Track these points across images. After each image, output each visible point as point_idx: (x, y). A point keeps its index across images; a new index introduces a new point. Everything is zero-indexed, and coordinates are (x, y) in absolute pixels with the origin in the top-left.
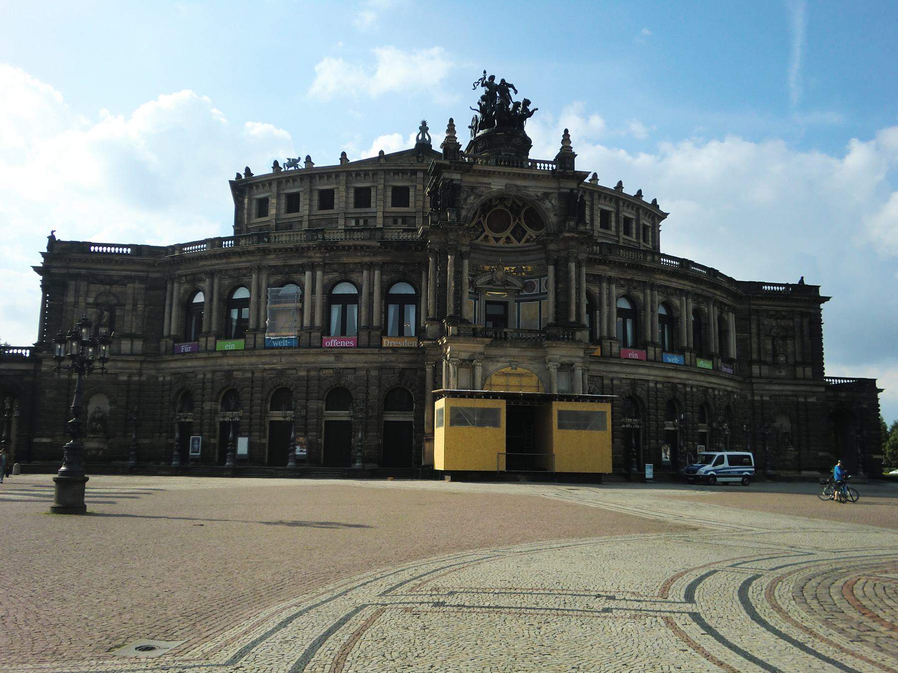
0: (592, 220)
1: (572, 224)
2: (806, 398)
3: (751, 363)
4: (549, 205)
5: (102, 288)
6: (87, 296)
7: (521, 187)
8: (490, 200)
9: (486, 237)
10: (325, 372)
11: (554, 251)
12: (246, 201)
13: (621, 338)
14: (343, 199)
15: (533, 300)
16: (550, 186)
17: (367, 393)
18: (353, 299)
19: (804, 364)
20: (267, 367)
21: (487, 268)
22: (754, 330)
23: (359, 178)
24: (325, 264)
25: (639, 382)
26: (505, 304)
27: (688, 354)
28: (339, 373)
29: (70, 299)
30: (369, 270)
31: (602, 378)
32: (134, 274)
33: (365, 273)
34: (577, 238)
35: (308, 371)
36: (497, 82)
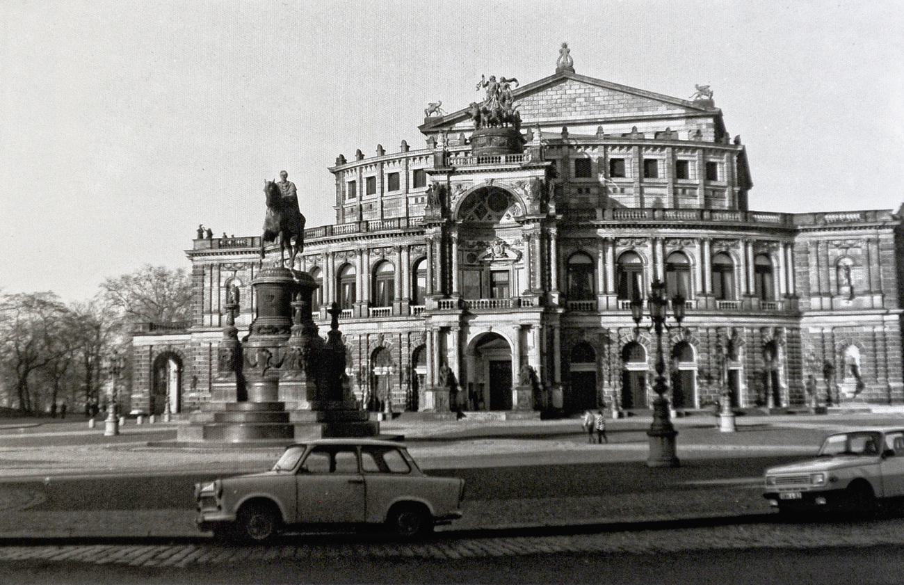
1: (537, 208)
2: (874, 328)
3: (810, 295)
4: (520, 191)
5: (230, 274)
6: (219, 281)
17: (401, 352)
19: (870, 293)
22: (813, 262)
24: (369, 249)
26: (507, 271)
27: (702, 300)
28: (382, 337)
29: (207, 285)
32: (251, 261)
34: (538, 220)
35: (360, 336)
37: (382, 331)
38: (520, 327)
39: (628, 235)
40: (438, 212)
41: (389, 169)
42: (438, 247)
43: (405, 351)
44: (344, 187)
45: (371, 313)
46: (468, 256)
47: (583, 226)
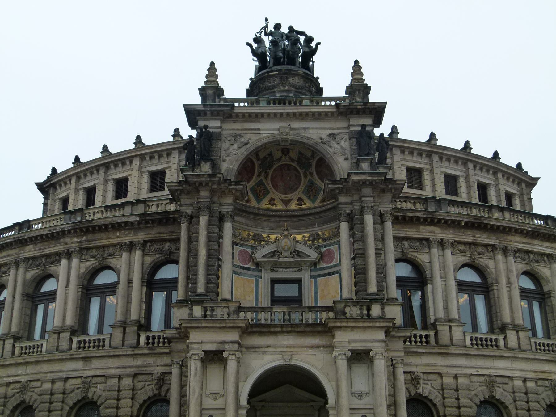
0: (433, 185)
1: (365, 166)
7: (298, 129)
8: (270, 155)
9: (272, 200)
10: (71, 381)
11: (346, 204)
12: (50, 201)
13: (467, 319)
14: (138, 187)
15: (333, 273)
16: (337, 126)
17: (117, 408)
18: (111, 289)
20: (12, 379)
21: (273, 237)
23: (154, 161)
25: (498, 380)
26: (299, 281)
28: (87, 384)
30: (127, 251)
31: (439, 374)
33: (125, 255)
34: (371, 183)
35: (53, 382)
36: (285, 30)
37: (91, 373)
38: (350, 353)
39: (470, 239)
40: (206, 168)
41: (118, 173)
42: (203, 220)
43: (126, 403)
44: (53, 205)
45: (75, 344)
46: (241, 251)
47: (411, 218)
